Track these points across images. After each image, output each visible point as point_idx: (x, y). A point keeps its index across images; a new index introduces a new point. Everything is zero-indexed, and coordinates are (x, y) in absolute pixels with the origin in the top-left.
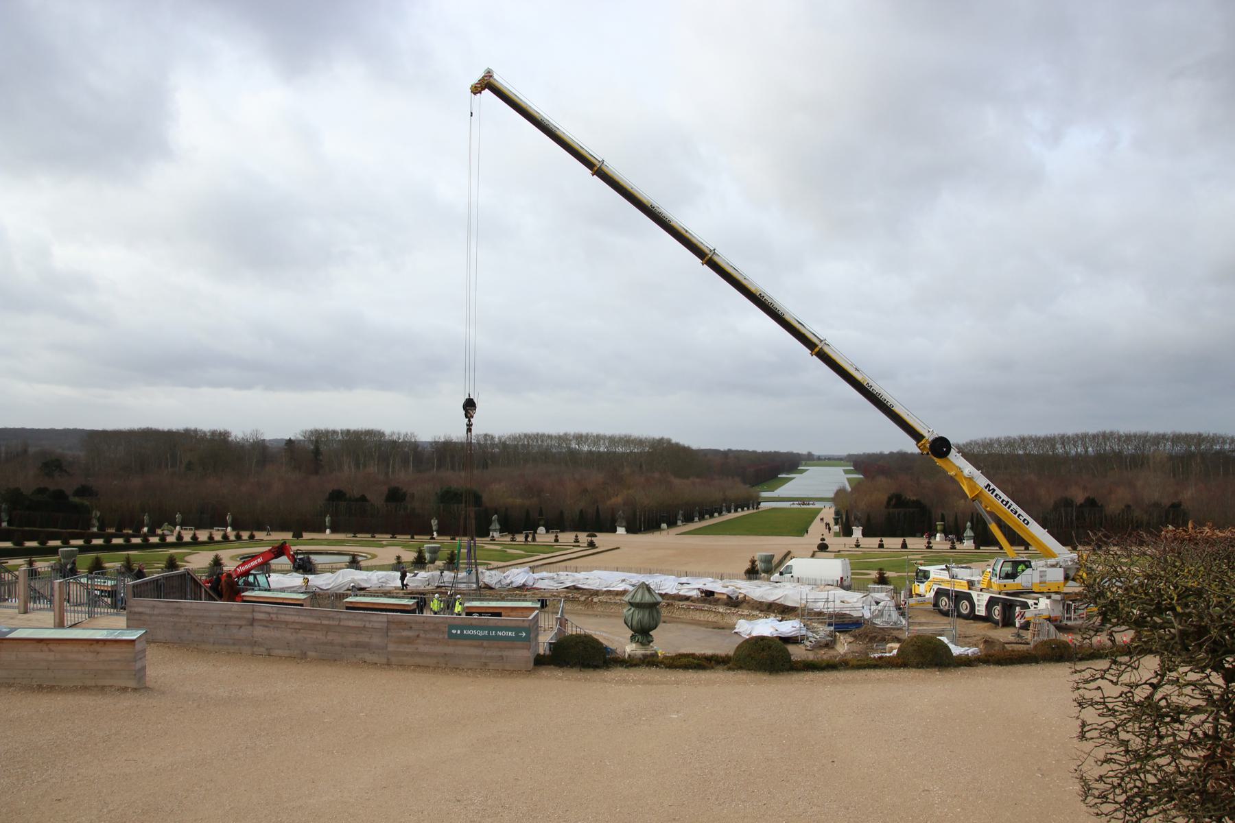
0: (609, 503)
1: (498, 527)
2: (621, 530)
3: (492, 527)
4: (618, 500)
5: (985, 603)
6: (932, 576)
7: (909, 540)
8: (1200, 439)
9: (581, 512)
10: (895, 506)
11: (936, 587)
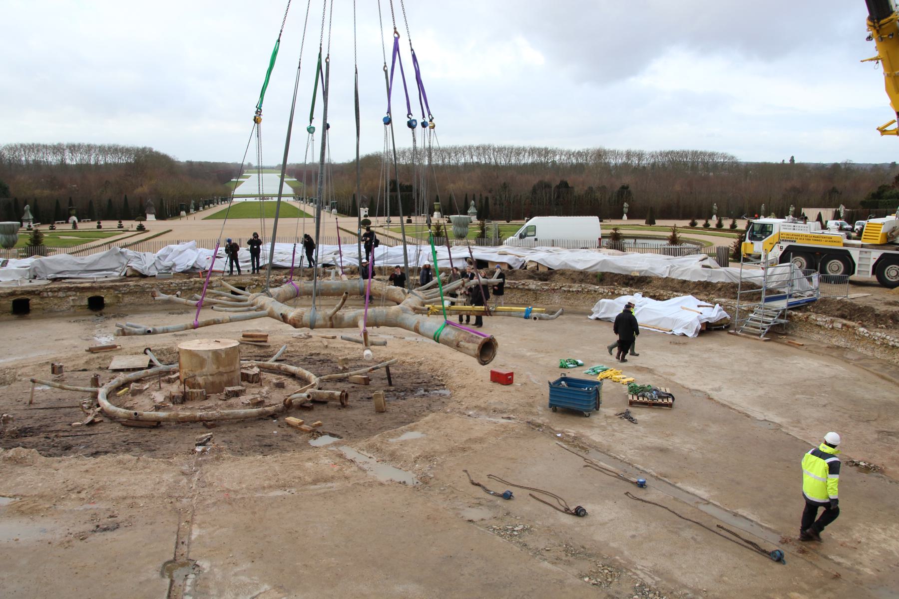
0: (139, 190)
1: (31, 217)
2: (151, 217)
3: (25, 217)
4: (143, 189)
5: (873, 262)
6: (775, 231)
7: (413, 218)
8: (547, 152)
9: (110, 201)
11: (785, 245)
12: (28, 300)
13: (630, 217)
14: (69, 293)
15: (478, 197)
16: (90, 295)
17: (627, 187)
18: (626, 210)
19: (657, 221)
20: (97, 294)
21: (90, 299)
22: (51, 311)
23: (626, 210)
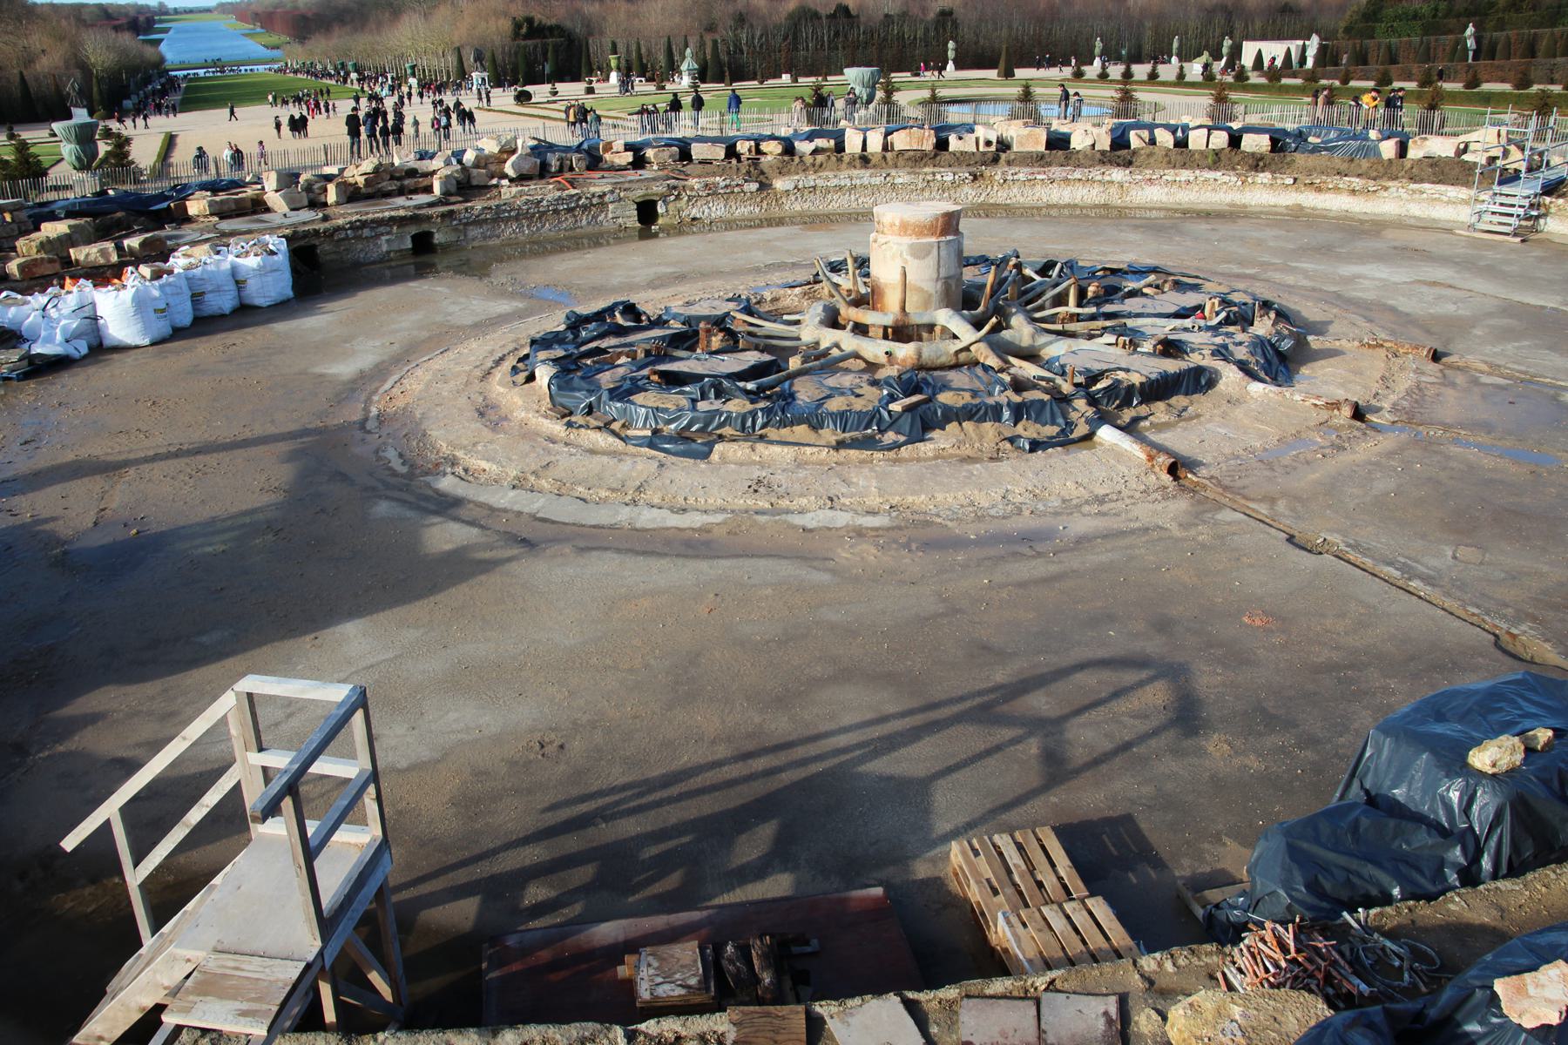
10: (526, 37)
12: (314, 247)
13: (959, 66)
14: (382, 229)
15: (693, 41)
16: (414, 230)
17: (951, 13)
18: (951, 54)
19: (1016, 71)
20: (425, 227)
21: (414, 238)
22: (357, 265)
23: (951, 54)
